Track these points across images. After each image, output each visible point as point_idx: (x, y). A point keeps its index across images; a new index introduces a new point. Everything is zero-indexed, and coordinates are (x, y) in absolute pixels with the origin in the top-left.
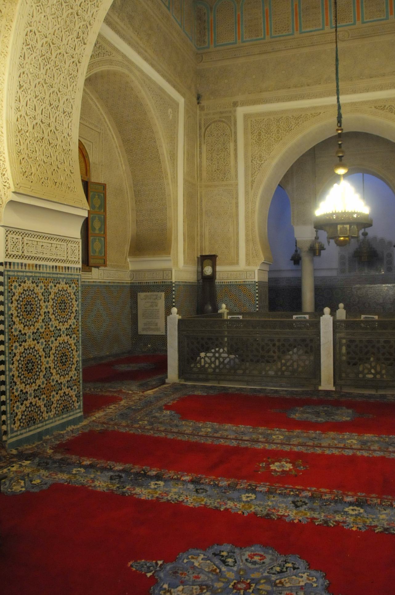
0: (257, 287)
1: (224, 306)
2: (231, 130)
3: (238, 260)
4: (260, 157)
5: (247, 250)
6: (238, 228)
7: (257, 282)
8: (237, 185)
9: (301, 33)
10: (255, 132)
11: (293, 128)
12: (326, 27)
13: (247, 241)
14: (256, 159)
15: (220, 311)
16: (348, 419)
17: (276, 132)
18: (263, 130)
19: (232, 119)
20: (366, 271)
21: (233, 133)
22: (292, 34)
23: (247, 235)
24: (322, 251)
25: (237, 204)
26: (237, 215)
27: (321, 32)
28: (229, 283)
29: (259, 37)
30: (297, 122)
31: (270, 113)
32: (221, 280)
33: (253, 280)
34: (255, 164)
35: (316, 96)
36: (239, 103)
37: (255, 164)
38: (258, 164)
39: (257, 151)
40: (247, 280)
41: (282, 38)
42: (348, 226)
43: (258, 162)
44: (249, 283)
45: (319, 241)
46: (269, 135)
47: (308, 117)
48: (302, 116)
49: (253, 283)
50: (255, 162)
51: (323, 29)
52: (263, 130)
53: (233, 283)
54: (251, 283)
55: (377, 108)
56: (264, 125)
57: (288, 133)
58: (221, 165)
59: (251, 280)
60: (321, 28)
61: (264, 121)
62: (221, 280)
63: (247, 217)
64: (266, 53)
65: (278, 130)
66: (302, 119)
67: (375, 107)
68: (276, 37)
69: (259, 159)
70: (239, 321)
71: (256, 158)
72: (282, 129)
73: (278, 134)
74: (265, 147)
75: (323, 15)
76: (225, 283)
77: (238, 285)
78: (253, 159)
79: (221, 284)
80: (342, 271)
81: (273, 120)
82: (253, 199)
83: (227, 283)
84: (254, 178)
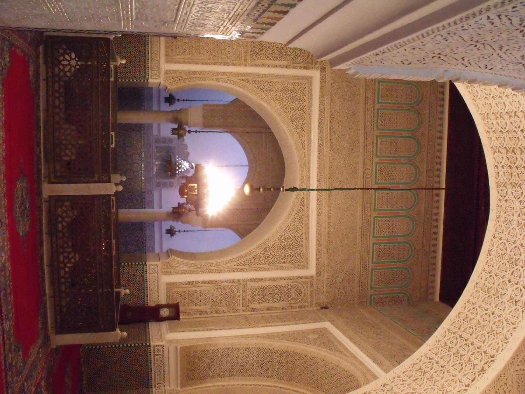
0: (142, 81)
1: (124, 62)
2: (299, 63)
3: (170, 62)
4: (270, 90)
5: (181, 72)
6: (202, 63)
7: (147, 81)
8: (246, 65)
9: (377, 137)
10: (295, 87)
11: (294, 123)
12: (378, 159)
13: (190, 72)
14: (269, 86)
15: (119, 59)
16: (21, 234)
17: (292, 106)
18: (296, 94)
19: (310, 66)
20: (157, 163)
21: (296, 65)
22: (377, 129)
23: (195, 72)
24: (176, 136)
25: (228, 64)
26: (215, 64)
27: (374, 155)
28: (147, 52)
29: (380, 98)
30: (299, 127)
31: (310, 103)
32: (151, 42)
33: (150, 77)
34: (264, 85)
35: (320, 146)
36: (323, 74)
37: (264, 85)
38: (263, 87)
39: (276, 87)
40: (150, 71)
41: (376, 118)
42: (196, 193)
43: (266, 87)
44: (147, 73)
45: (187, 133)
46: (290, 100)
47: (302, 138)
48: (303, 132)
49: (147, 77)
50: (266, 84)
51: (377, 156)
52: (296, 94)
53: (147, 56)
54: (147, 75)
55: (302, 199)
56: (300, 96)
57: (289, 118)
58: (267, 51)
59: (150, 75)
60: (378, 154)
61: (304, 96)
62: (151, 42)
63: (212, 73)
64: (366, 103)
65: (293, 109)
66: (301, 132)
67: (303, 198)
68: (378, 113)
69: (269, 89)
70: (109, 77)
71: (270, 86)
72: (294, 113)
73: (289, 109)
74: (280, 95)
75: (389, 157)
76: (147, 48)
77: (145, 60)
78: (269, 83)
79: (147, 43)
80: (157, 140)
81: (304, 105)
82: (230, 80)
83: (147, 50)
84: (250, 82)
